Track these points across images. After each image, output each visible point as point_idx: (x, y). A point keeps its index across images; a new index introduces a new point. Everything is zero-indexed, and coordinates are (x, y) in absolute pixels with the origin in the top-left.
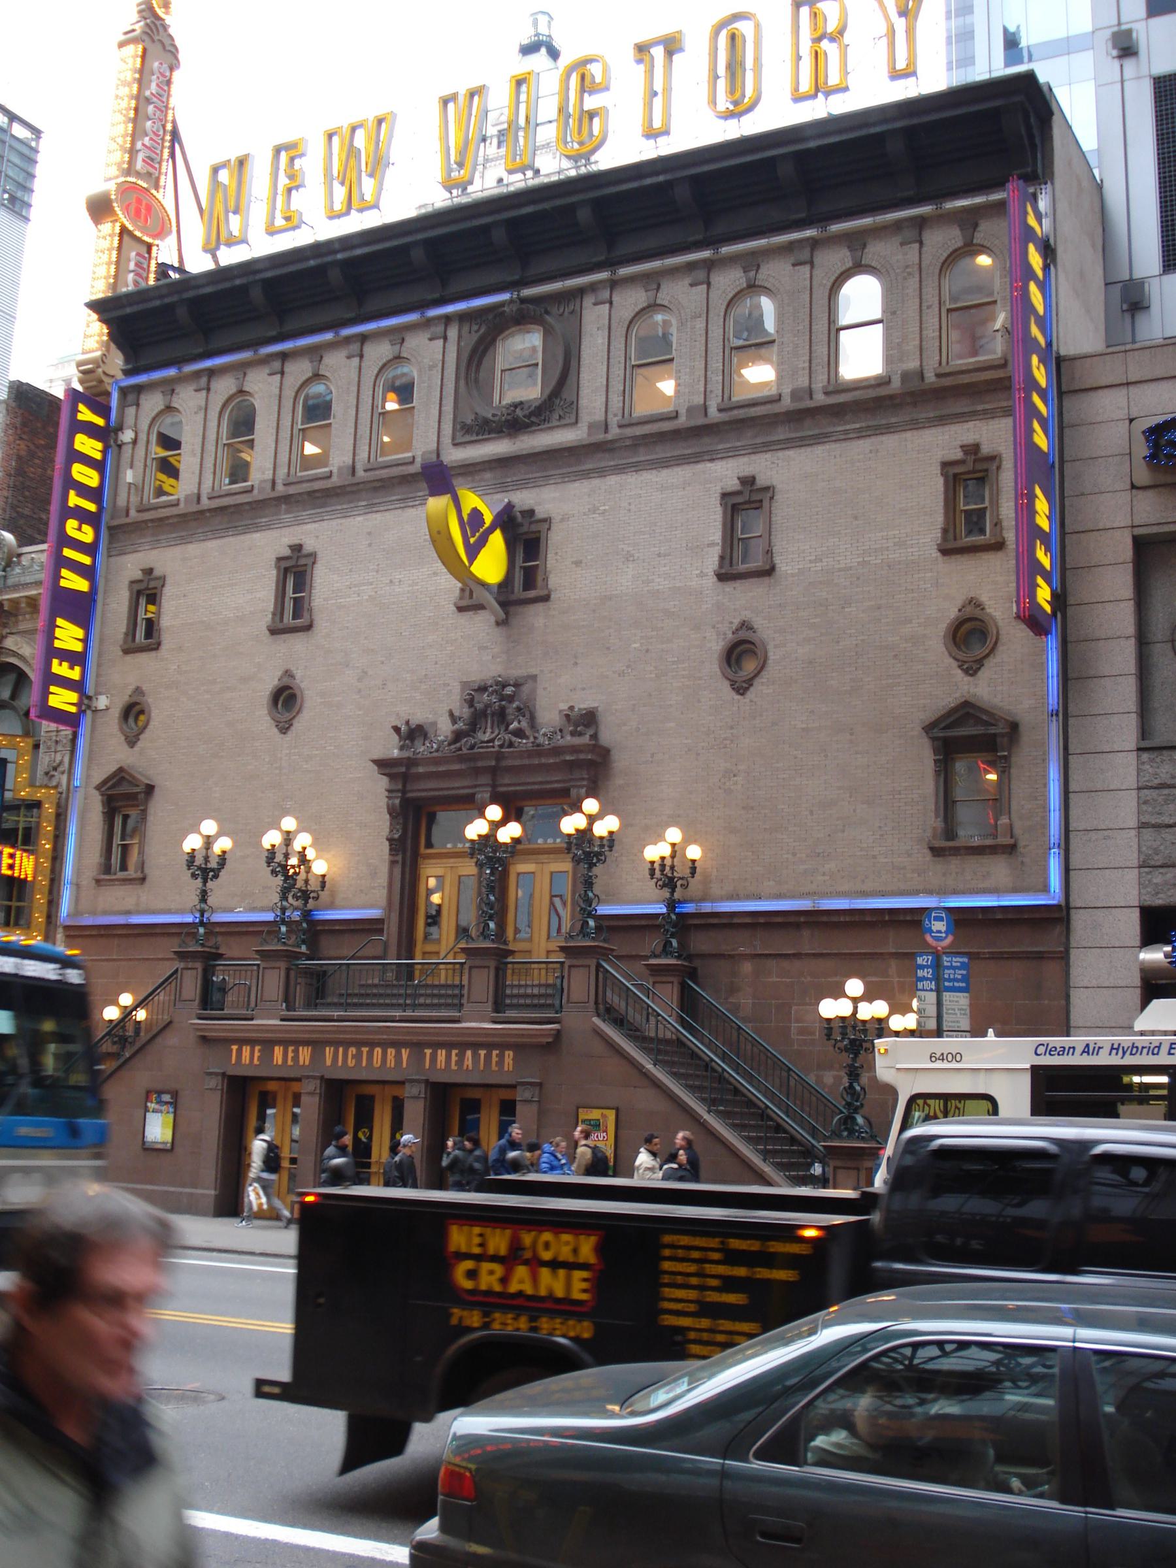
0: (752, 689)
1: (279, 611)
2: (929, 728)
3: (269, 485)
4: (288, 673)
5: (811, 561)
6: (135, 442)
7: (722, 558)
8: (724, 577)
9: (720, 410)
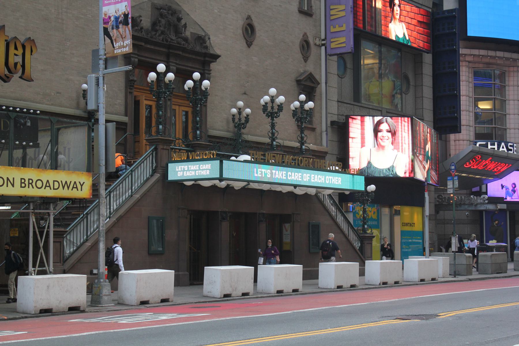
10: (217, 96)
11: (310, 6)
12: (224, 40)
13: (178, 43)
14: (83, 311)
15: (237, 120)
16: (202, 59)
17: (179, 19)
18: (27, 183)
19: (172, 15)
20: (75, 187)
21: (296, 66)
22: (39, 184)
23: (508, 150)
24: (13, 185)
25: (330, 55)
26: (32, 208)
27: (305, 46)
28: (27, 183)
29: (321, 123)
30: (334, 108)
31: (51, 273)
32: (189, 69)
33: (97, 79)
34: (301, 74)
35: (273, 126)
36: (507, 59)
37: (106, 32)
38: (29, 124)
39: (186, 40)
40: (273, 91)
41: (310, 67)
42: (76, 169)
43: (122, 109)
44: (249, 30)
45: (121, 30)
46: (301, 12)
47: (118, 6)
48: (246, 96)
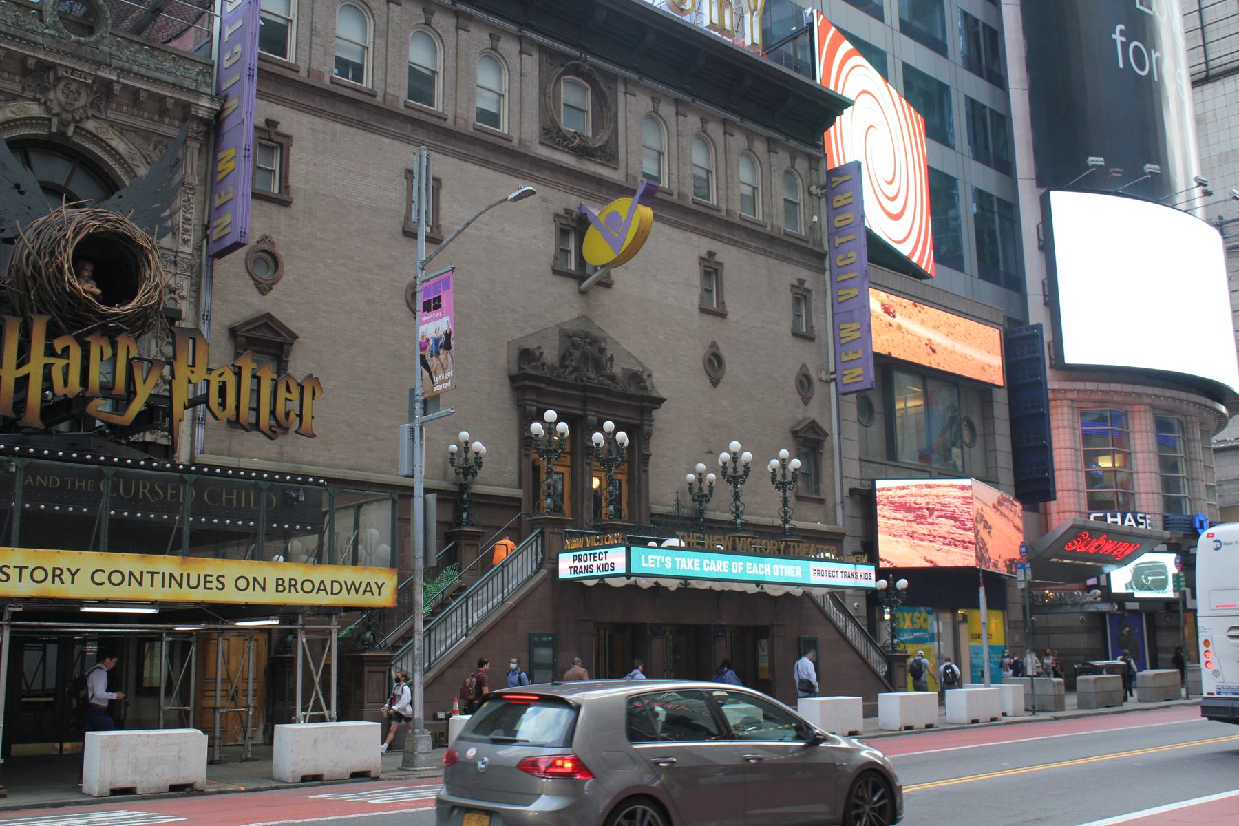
11: (810, 327)
12: (674, 379)
13: (600, 383)
14: (377, 779)
15: (696, 491)
17: (602, 350)
18: (287, 584)
19: (590, 344)
20: (368, 589)
21: (792, 412)
22: (308, 586)
23: (1138, 523)
24: (264, 589)
25: (844, 394)
26: (300, 621)
27: (804, 383)
28: (287, 584)
29: (834, 491)
30: (853, 469)
31: (331, 720)
33: (412, 431)
34: (801, 422)
36: (1128, 394)
37: (424, 363)
38: (302, 499)
39: (613, 378)
40: (735, 445)
41: (813, 412)
42: (379, 564)
43: (515, 478)
44: (714, 363)
45: (442, 357)
46: (796, 334)
47: (439, 323)
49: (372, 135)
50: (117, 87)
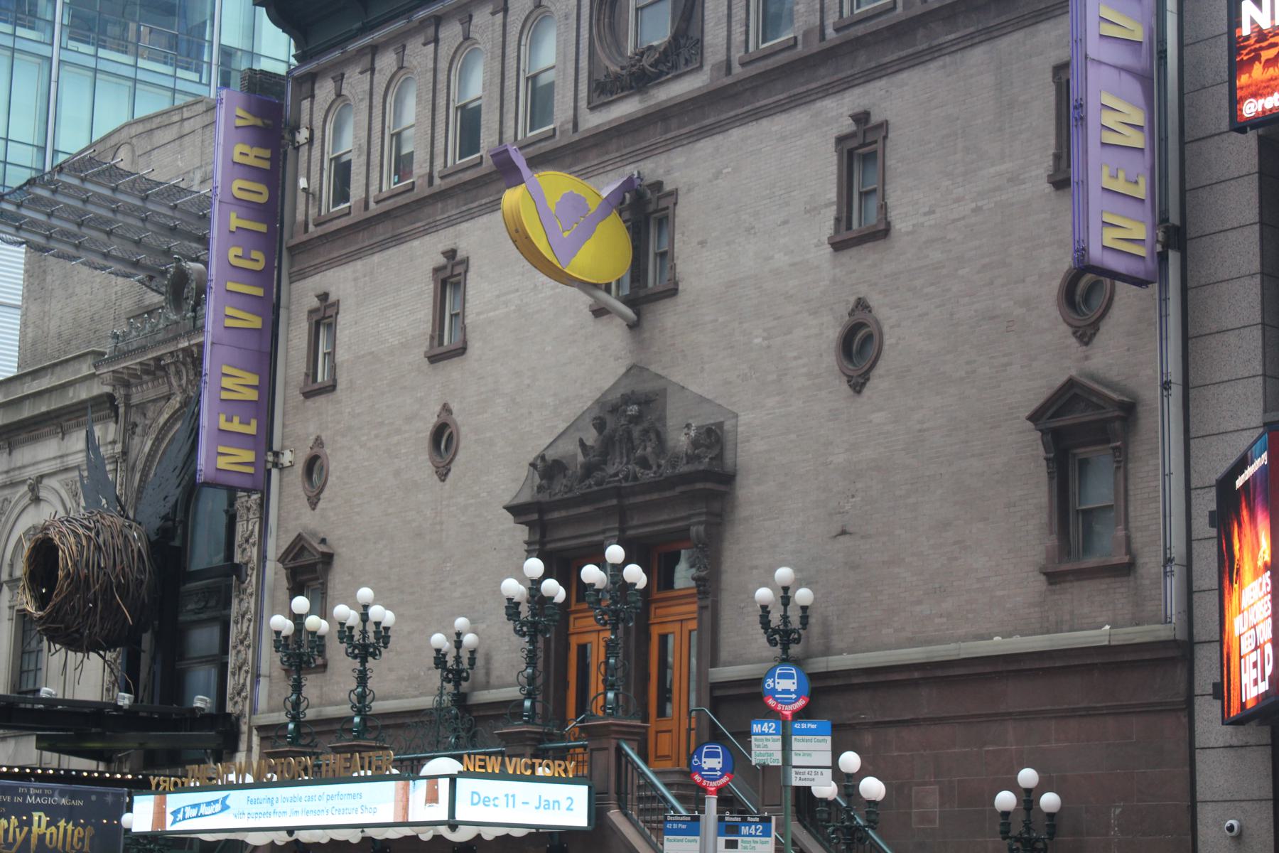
0: (868, 384)
1: (843, 219)
2: (1034, 418)
3: (570, 126)
4: (861, 305)
5: (925, 214)
6: (311, 141)
7: (838, 220)
8: (839, 246)
9: (837, 30)
10: (756, 567)
16: (614, 502)
32: (662, 527)
35: (362, 678)
48: (847, 537)
49: (404, 247)
50: (195, 349)
